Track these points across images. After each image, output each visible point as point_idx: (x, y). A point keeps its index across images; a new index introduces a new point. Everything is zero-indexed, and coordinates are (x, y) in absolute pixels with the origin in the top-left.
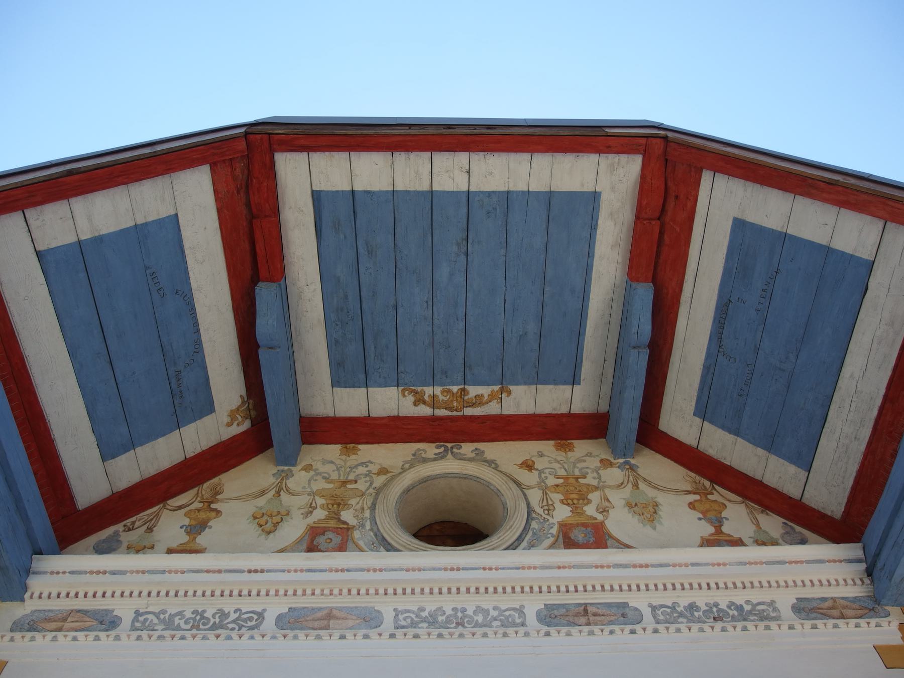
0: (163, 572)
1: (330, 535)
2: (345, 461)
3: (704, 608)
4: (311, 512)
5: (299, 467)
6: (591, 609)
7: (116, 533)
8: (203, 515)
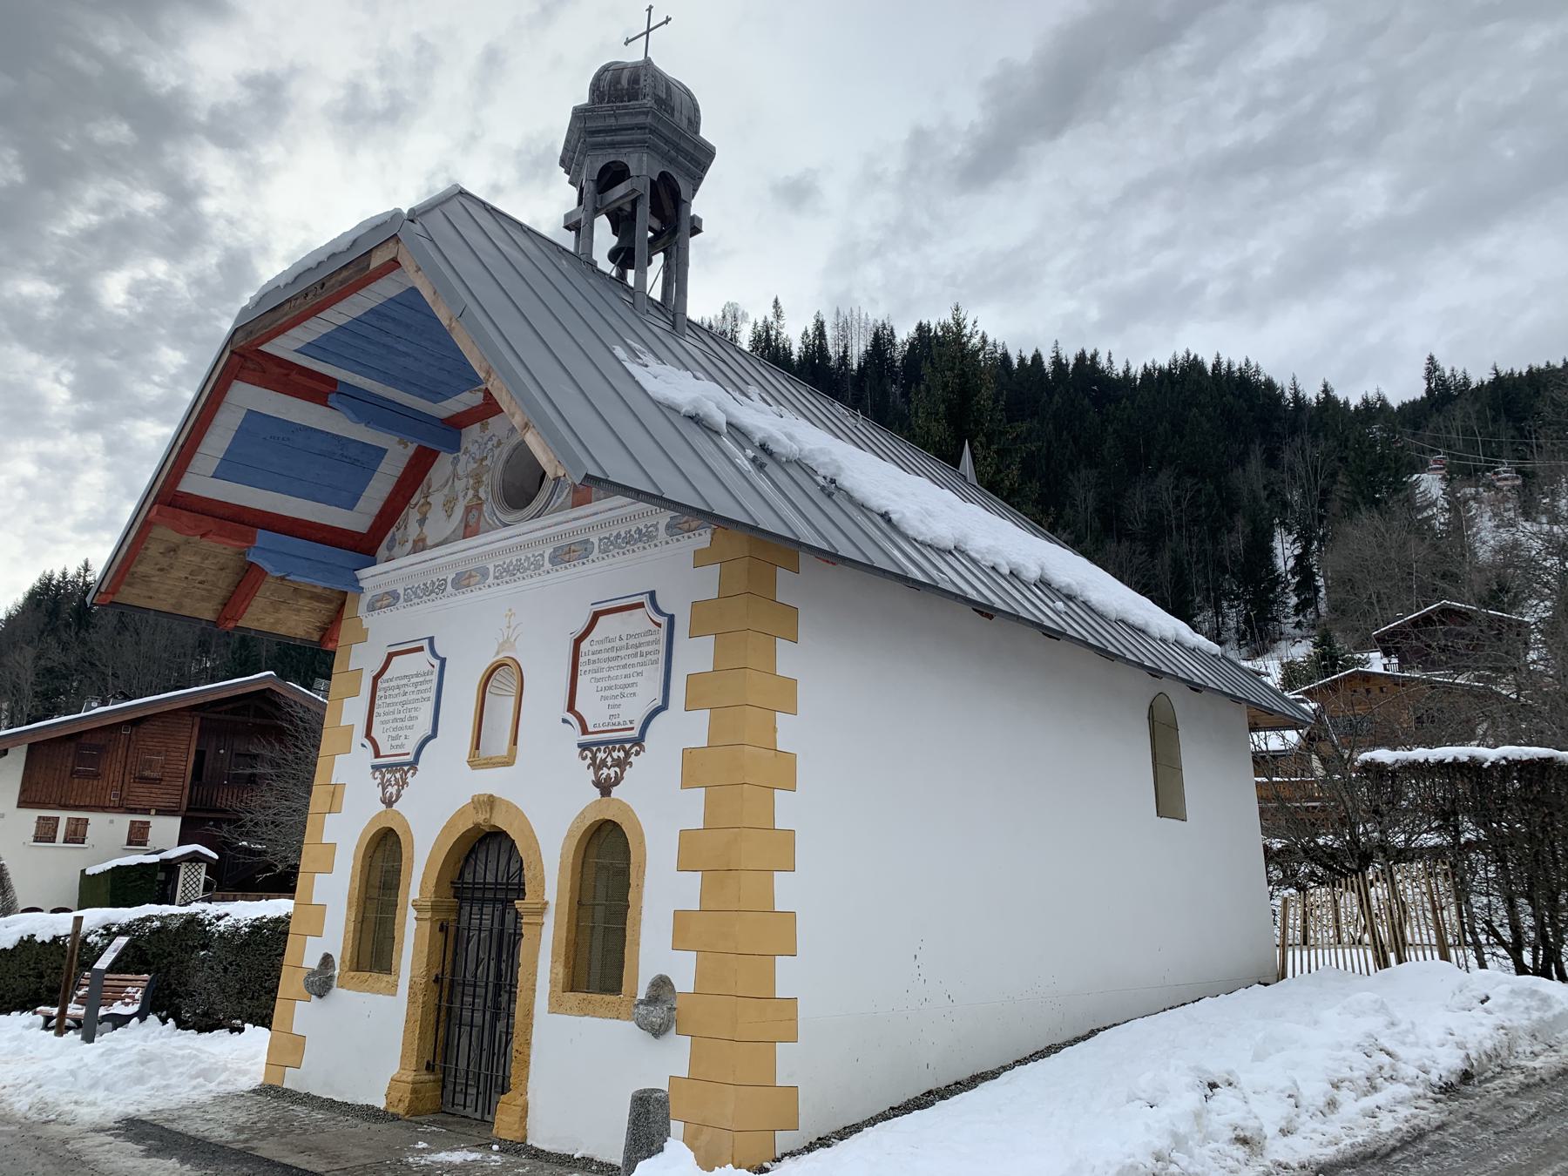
0: (401, 568)
1: (474, 512)
2: (482, 438)
3: (623, 535)
4: (466, 494)
5: (462, 451)
6: (573, 547)
7: (394, 534)
8: (424, 509)
